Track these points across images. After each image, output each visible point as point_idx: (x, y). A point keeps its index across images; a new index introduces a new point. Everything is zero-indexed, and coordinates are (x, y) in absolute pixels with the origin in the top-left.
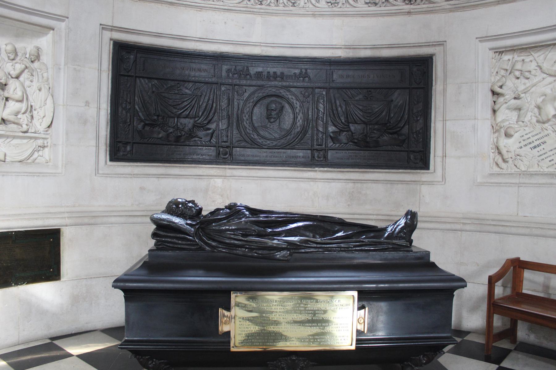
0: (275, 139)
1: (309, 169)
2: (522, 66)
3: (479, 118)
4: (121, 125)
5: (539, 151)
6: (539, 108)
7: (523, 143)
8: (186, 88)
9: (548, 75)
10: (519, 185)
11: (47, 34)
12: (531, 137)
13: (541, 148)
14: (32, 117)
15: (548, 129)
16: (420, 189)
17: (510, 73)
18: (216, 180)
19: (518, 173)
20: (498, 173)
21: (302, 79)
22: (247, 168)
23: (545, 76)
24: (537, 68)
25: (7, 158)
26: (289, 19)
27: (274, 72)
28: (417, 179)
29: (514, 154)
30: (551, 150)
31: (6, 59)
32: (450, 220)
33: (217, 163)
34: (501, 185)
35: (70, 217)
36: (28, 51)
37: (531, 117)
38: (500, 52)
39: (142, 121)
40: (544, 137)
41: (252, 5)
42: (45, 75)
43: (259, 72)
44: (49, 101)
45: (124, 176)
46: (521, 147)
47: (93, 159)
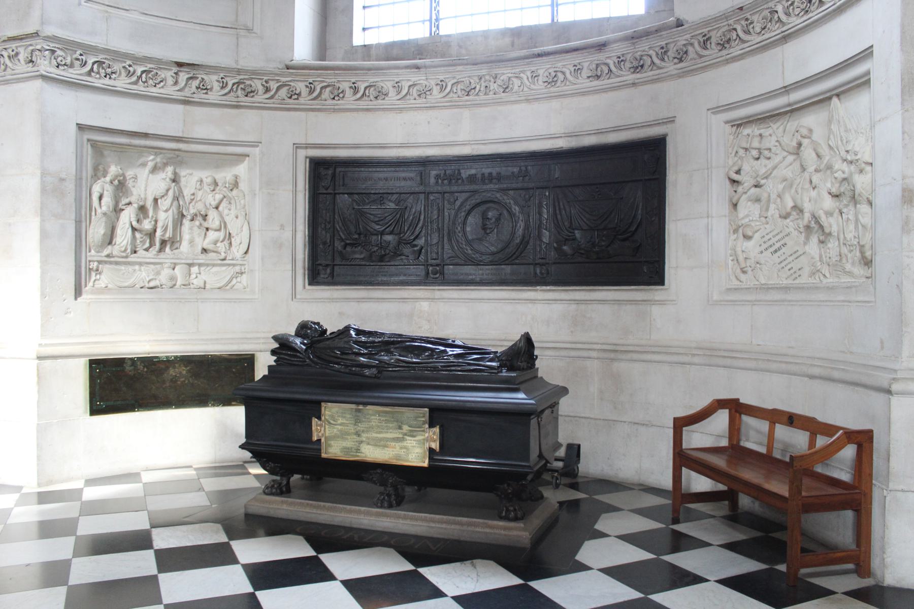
0: (493, 254)
1: (530, 288)
2: (760, 142)
4: (321, 246)
7: (764, 246)
8: (390, 201)
10: (753, 303)
11: (243, 161)
14: (231, 243)
16: (651, 311)
18: (422, 303)
20: (737, 287)
21: (521, 178)
22: (491, 289)
25: (206, 285)
26: (500, 108)
27: (489, 174)
28: (649, 298)
30: (791, 255)
31: (208, 190)
32: (681, 351)
33: (425, 284)
34: (737, 303)
35: (265, 343)
36: (228, 179)
38: (739, 124)
39: (342, 240)
41: (459, 97)
42: (242, 202)
43: (472, 175)
44: (246, 228)
45: (322, 300)
46: (762, 252)
47: (289, 284)
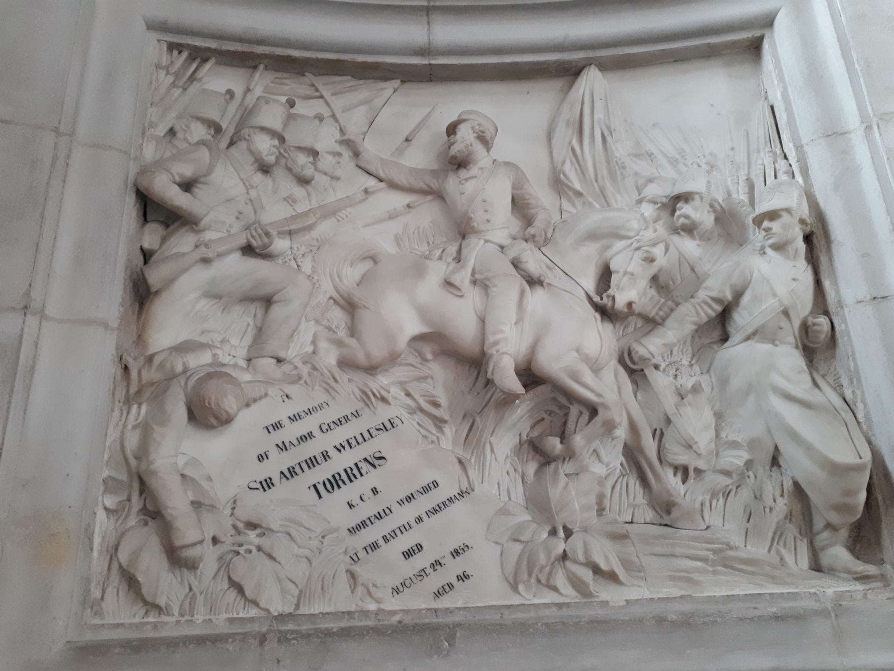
3: (50, 311)
5: (356, 500)
6: (350, 306)
7: (279, 462)
9: (383, 185)
12: (316, 432)
13: (362, 485)
15: (390, 399)
17: (232, 143)
19: (248, 628)
20: (134, 635)
23: (372, 182)
24: (338, 148)
29: (230, 521)
30: (410, 498)
37: (314, 342)
40: (374, 432)
46: (267, 484)
